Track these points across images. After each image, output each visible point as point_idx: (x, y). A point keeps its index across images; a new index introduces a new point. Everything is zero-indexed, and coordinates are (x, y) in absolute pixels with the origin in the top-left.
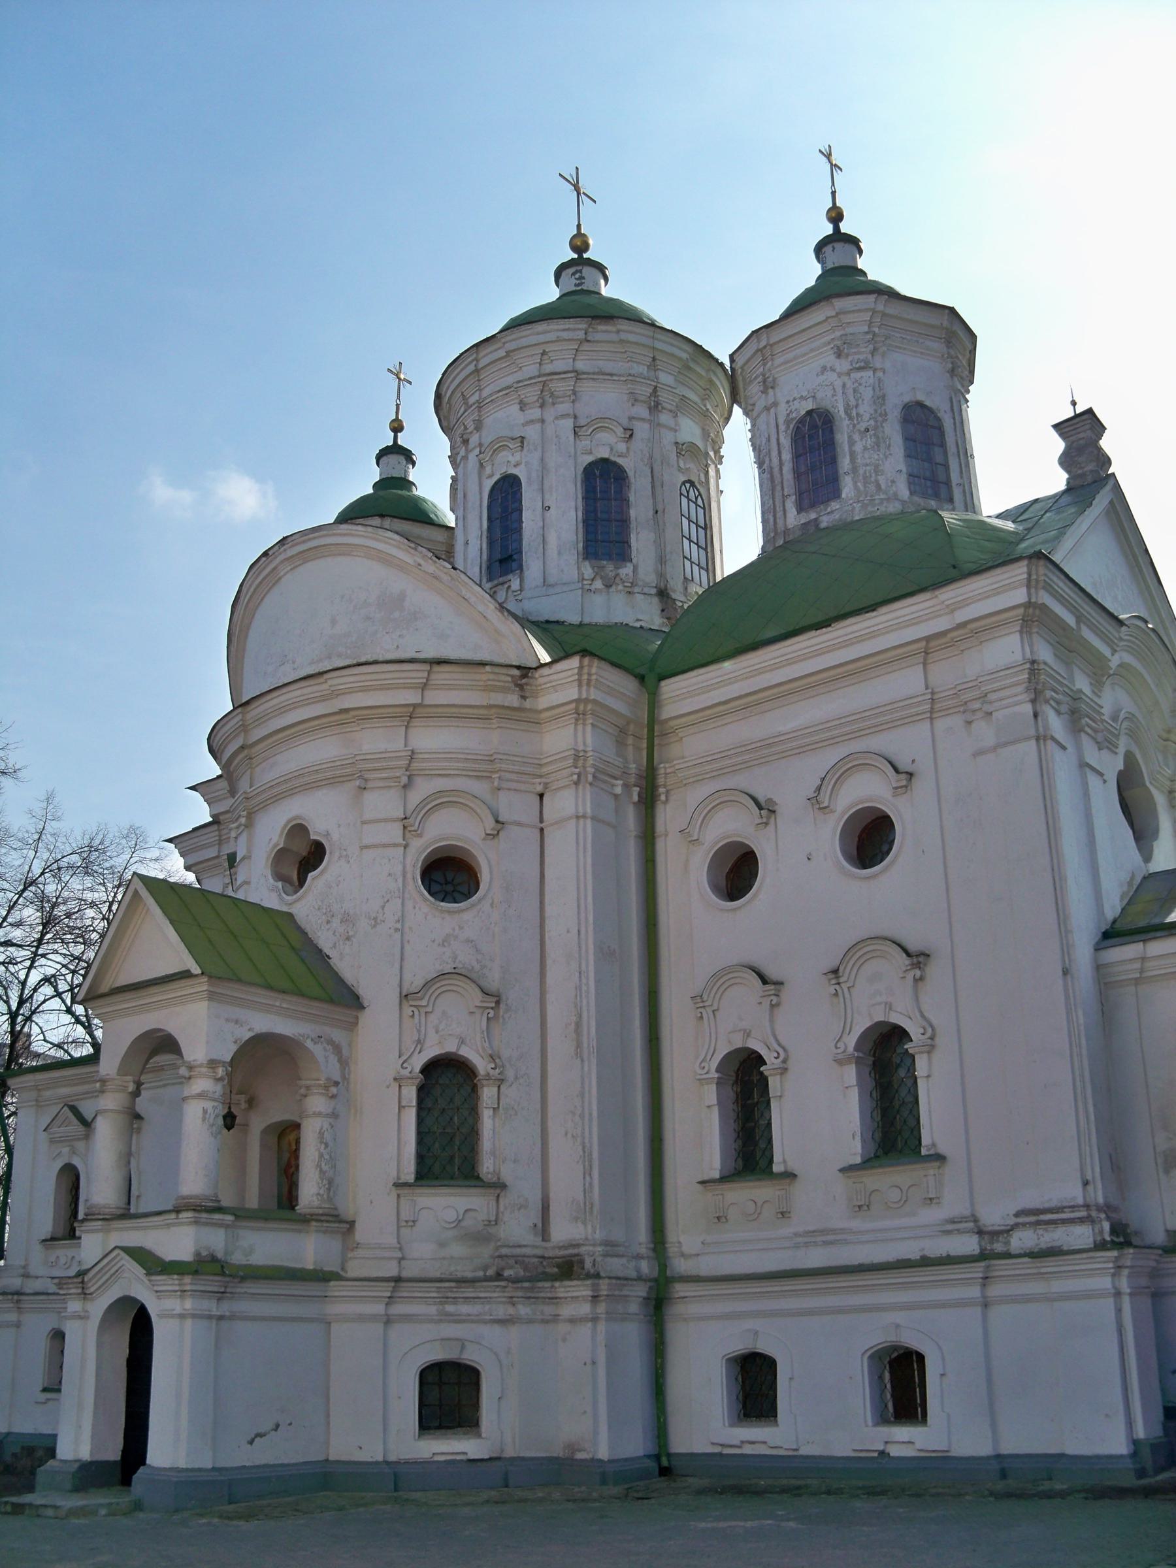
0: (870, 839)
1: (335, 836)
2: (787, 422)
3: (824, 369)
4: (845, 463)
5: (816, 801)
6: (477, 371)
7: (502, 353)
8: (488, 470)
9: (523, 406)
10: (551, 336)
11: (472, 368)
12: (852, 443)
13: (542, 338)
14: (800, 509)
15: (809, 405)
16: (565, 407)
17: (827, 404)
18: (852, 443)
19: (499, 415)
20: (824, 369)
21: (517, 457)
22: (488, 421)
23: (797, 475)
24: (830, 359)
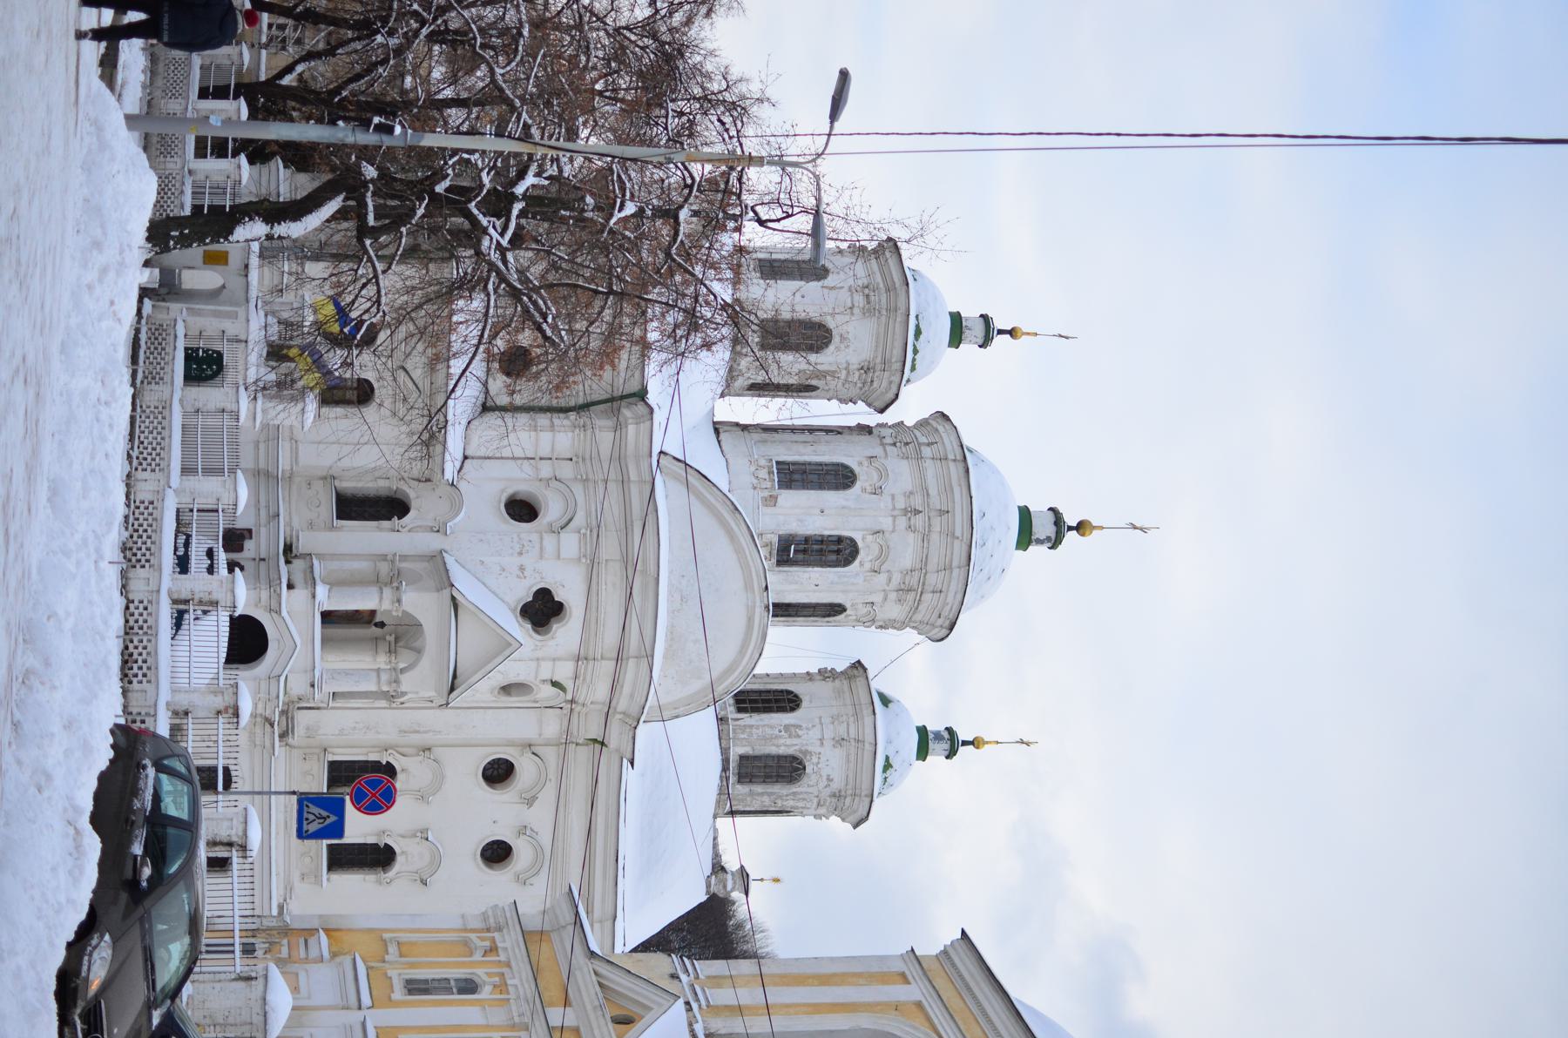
0: (497, 853)
1: (551, 643)
2: (806, 753)
3: (829, 779)
4: (758, 788)
5: (523, 830)
6: (954, 537)
7: (955, 564)
8: (870, 538)
10: (950, 599)
11: (958, 533)
12: (769, 794)
13: (951, 595)
14: (742, 757)
15: (808, 770)
16: (893, 596)
17: (805, 780)
18: (769, 794)
20: (829, 779)
21: (868, 566)
22: (911, 537)
23: (768, 756)
24: (835, 786)
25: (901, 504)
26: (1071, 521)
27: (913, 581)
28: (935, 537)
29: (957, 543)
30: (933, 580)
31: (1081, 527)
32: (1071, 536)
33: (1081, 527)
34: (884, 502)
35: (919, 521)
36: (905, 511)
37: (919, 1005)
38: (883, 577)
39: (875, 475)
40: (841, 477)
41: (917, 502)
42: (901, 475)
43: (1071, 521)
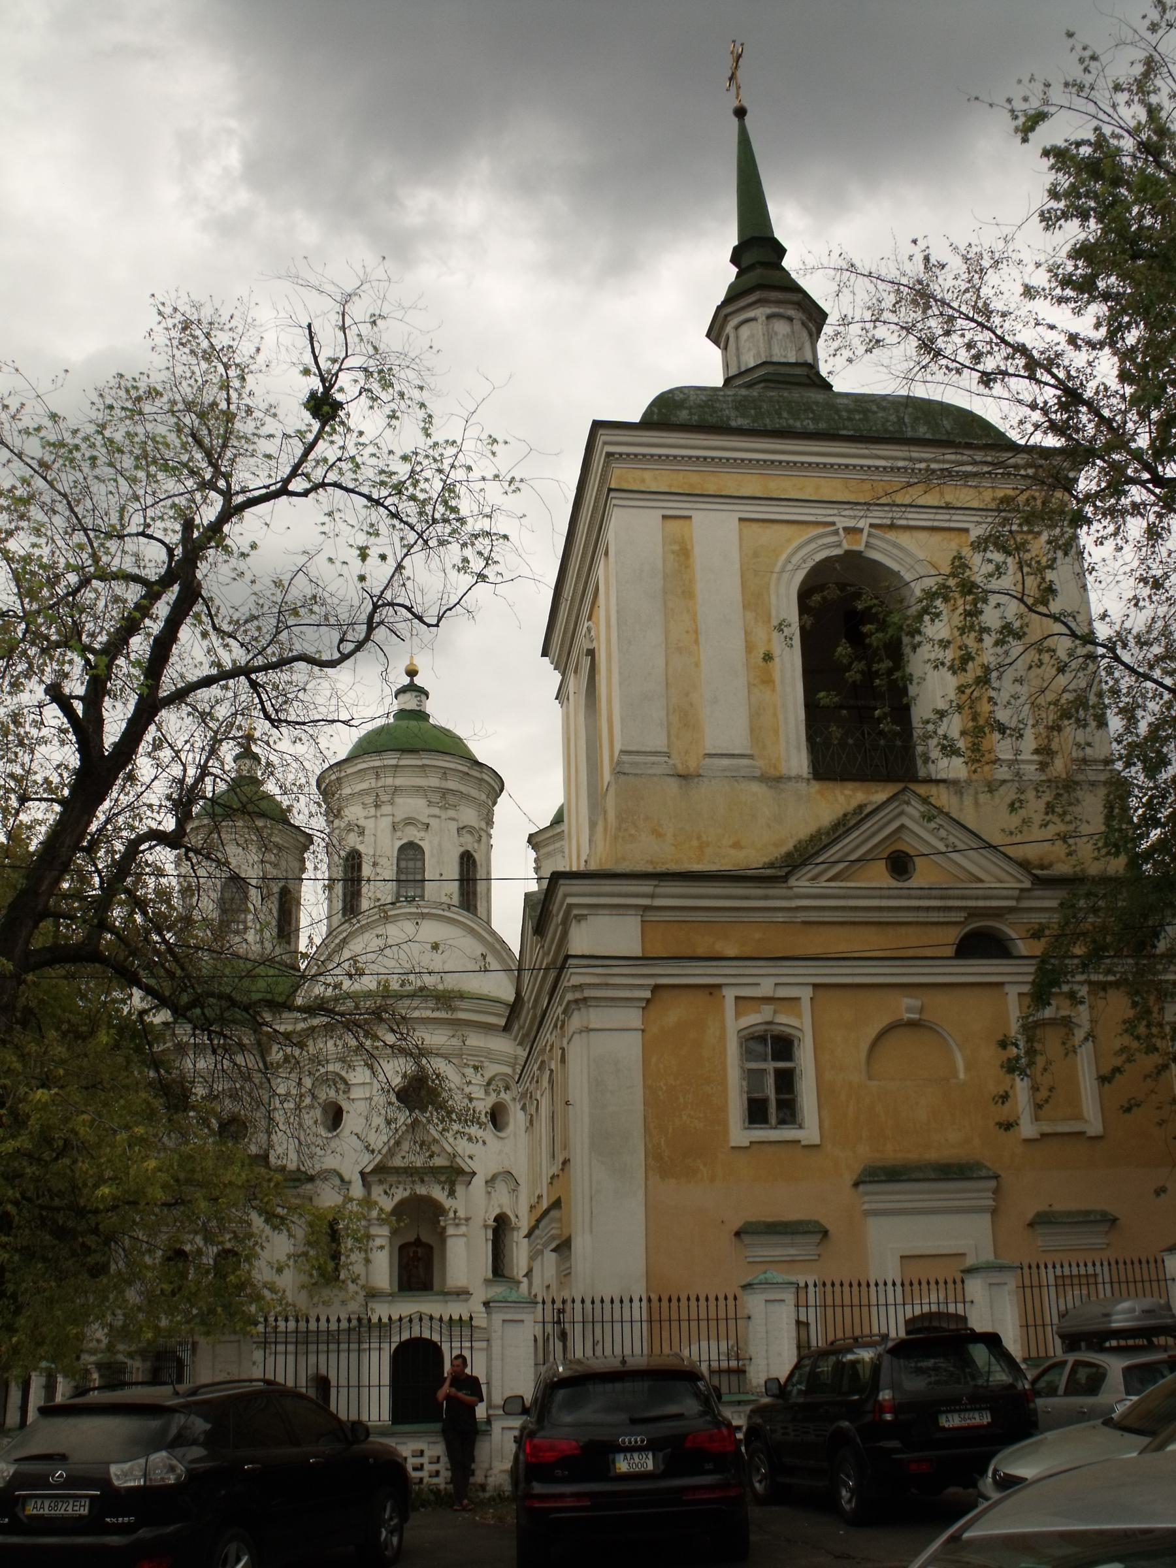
7: (419, 763)
8: (399, 834)
9: (430, 804)
16: (451, 813)
19: (409, 800)
21: (422, 834)
25: (372, 811)
26: (406, 680)
27: (435, 798)
28: (399, 782)
29: (402, 763)
30: (434, 781)
31: (412, 673)
32: (418, 681)
33: (412, 673)
34: (369, 825)
35: (384, 798)
36: (377, 806)
37: (576, 672)
38: (433, 822)
39: (352, 834)
40: (353, 861)
41: (370, 800)
42: (354, 812)
43: (406, 680)
